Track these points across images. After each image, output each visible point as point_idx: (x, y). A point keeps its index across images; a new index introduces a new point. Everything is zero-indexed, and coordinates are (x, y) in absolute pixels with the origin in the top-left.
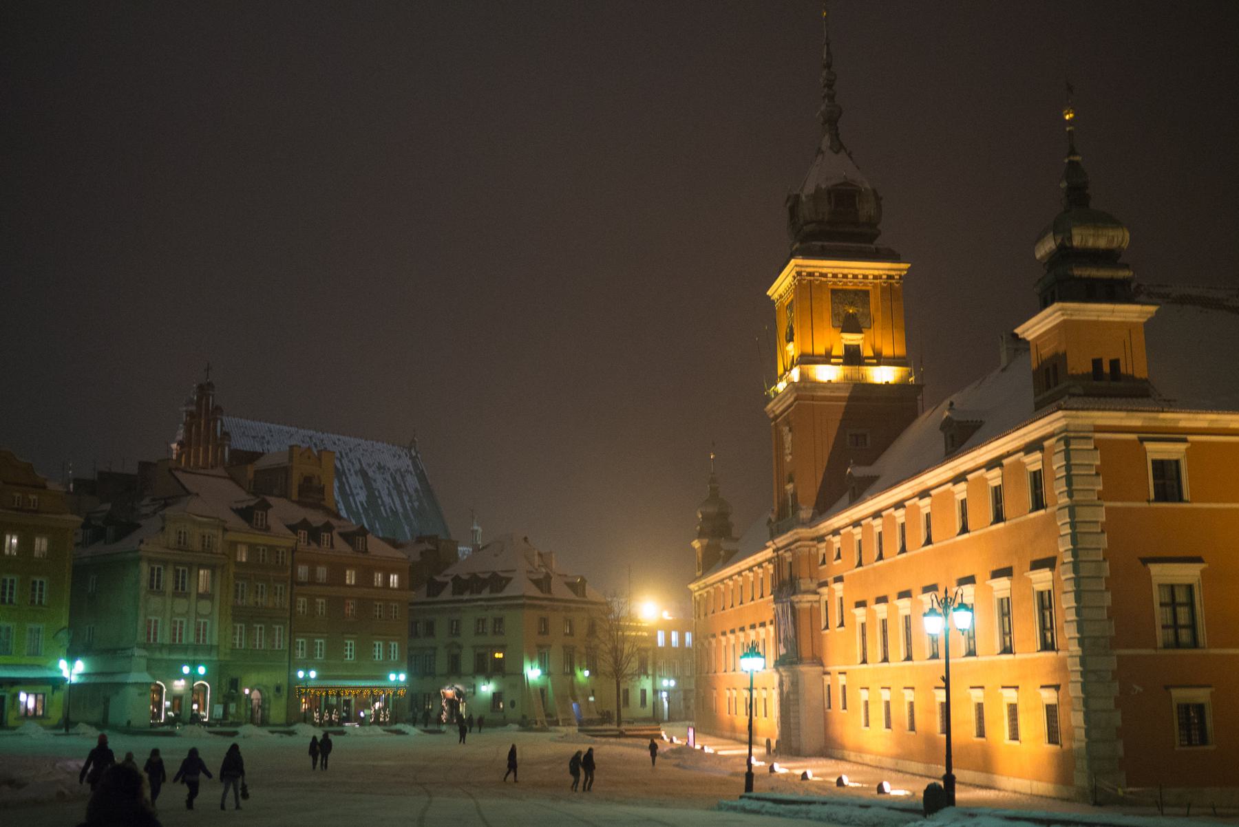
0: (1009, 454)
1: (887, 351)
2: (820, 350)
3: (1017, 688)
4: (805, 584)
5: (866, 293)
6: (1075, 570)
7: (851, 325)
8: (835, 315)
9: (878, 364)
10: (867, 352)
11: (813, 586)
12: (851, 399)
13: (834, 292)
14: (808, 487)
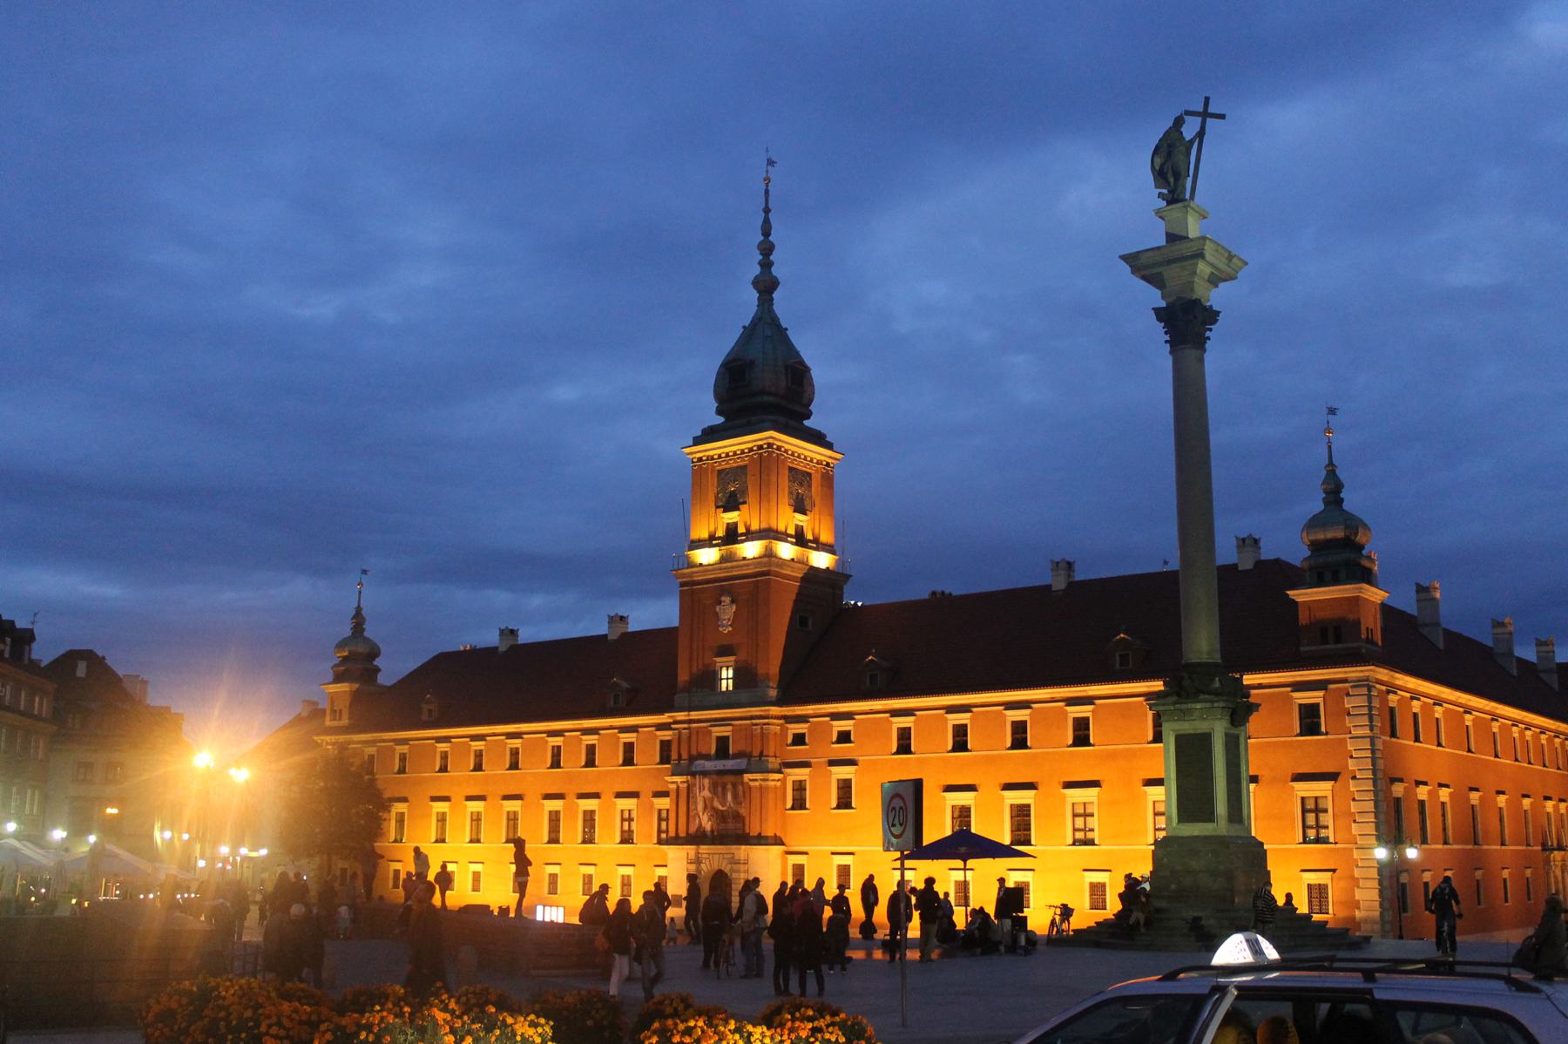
0: (1260, 686)
1: (826, 537)
2: (781, 528)
3: (1334, 871)
4: (773, 762)
5: (809, 475)
6: (1375, 785)
7: (800, 508)
8: (791, 493)
9: (816, 549)
10: (810, 536)
11: (777, 766)
12: (803, 579)
13: (791, 469)
14: (772, 663)
